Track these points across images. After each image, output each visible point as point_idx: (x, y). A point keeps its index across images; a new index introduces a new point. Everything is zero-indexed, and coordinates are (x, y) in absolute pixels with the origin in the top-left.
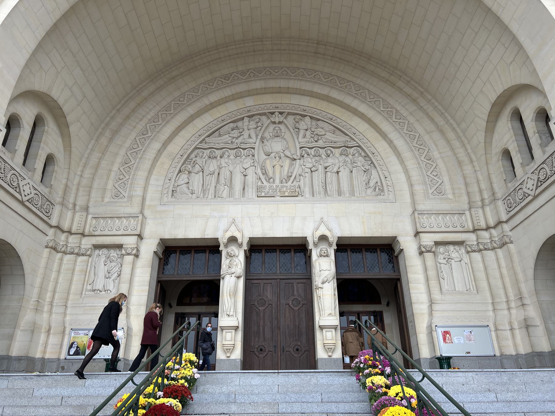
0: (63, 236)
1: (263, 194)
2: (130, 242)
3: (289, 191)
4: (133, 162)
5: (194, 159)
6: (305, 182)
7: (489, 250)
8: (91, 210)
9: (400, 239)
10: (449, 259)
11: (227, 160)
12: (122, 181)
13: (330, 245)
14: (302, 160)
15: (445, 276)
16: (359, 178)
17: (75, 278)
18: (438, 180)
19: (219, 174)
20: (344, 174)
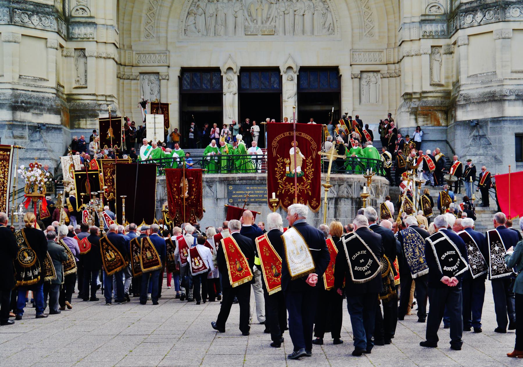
0: (122, 68)
1: (249, 33)
2: (162, 70)
3: (268, 30)
4: (155, 9)
5: (198, 3)
6: (279, 23)
7: (393, 77)
8: (133, 48)
9: (340, 67)
10: (368, 83)
11: (222, 5)
12: (149, 25)
13: (295, 73)
14: (278, 4)
15: (365, 93)
16: (318, 20)
17: (133, 94)
18: (371, 25)
19: (216, 15)
20: (308, 17)
